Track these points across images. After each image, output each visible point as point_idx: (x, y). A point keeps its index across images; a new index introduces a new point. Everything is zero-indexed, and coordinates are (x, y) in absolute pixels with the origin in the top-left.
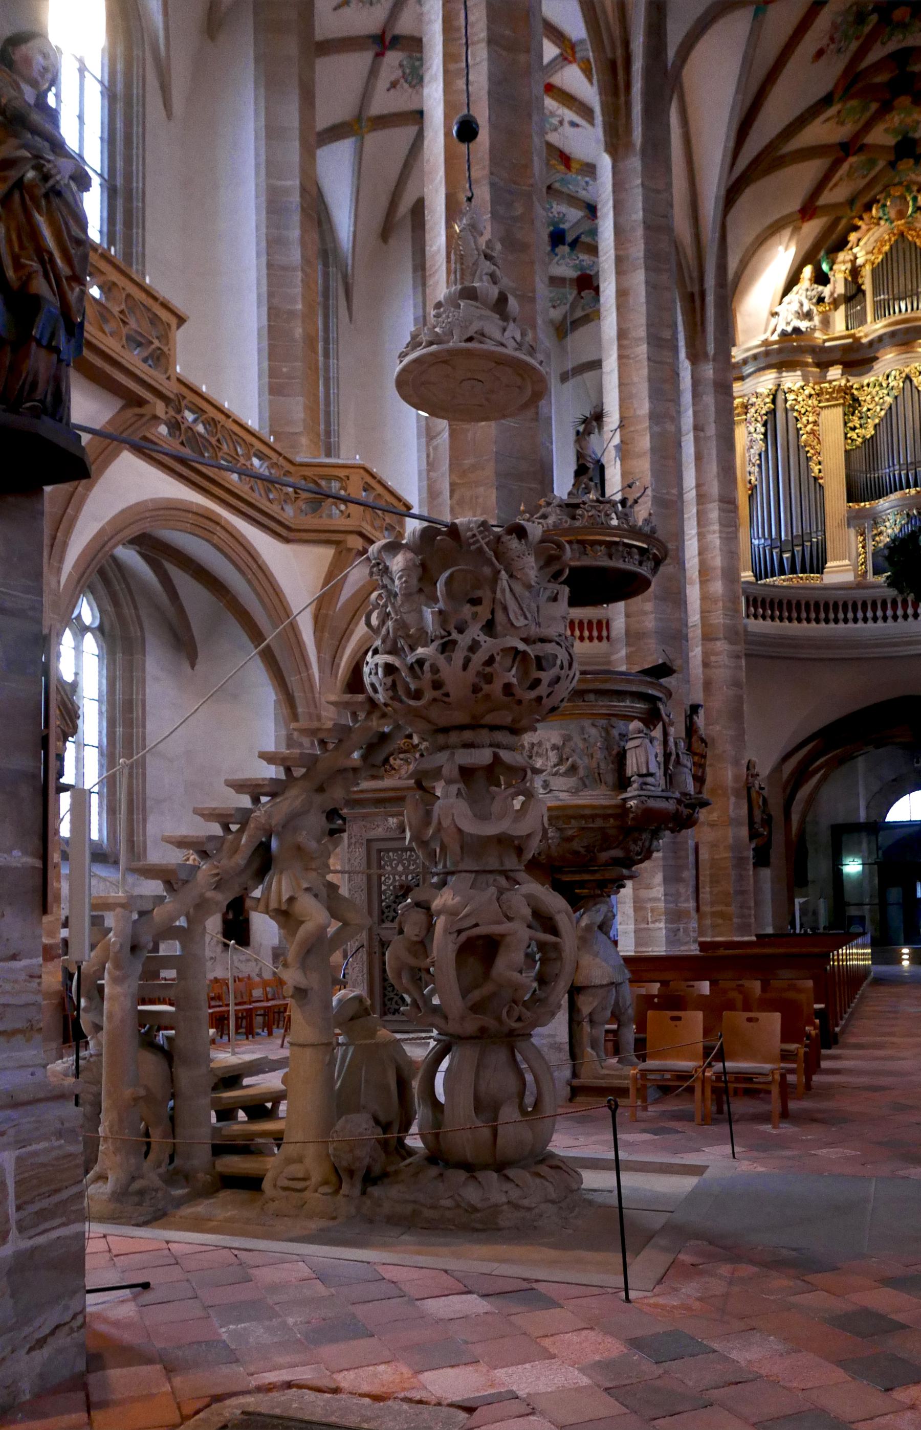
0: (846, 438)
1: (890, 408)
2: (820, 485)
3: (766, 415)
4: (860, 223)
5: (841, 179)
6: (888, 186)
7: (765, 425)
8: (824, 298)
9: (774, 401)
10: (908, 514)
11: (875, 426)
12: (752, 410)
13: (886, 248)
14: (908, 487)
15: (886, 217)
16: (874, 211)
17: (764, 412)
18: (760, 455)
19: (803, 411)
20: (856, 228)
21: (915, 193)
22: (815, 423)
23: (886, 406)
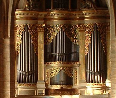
1: (56, 36)
3: (22, 32)
7: (22, 36)
9: (25, 29)
11: (52, 39)
12: (18, 30)
14: (60, 61)
17: (22, 31)
18: (20, 44)
23: (55, 35)
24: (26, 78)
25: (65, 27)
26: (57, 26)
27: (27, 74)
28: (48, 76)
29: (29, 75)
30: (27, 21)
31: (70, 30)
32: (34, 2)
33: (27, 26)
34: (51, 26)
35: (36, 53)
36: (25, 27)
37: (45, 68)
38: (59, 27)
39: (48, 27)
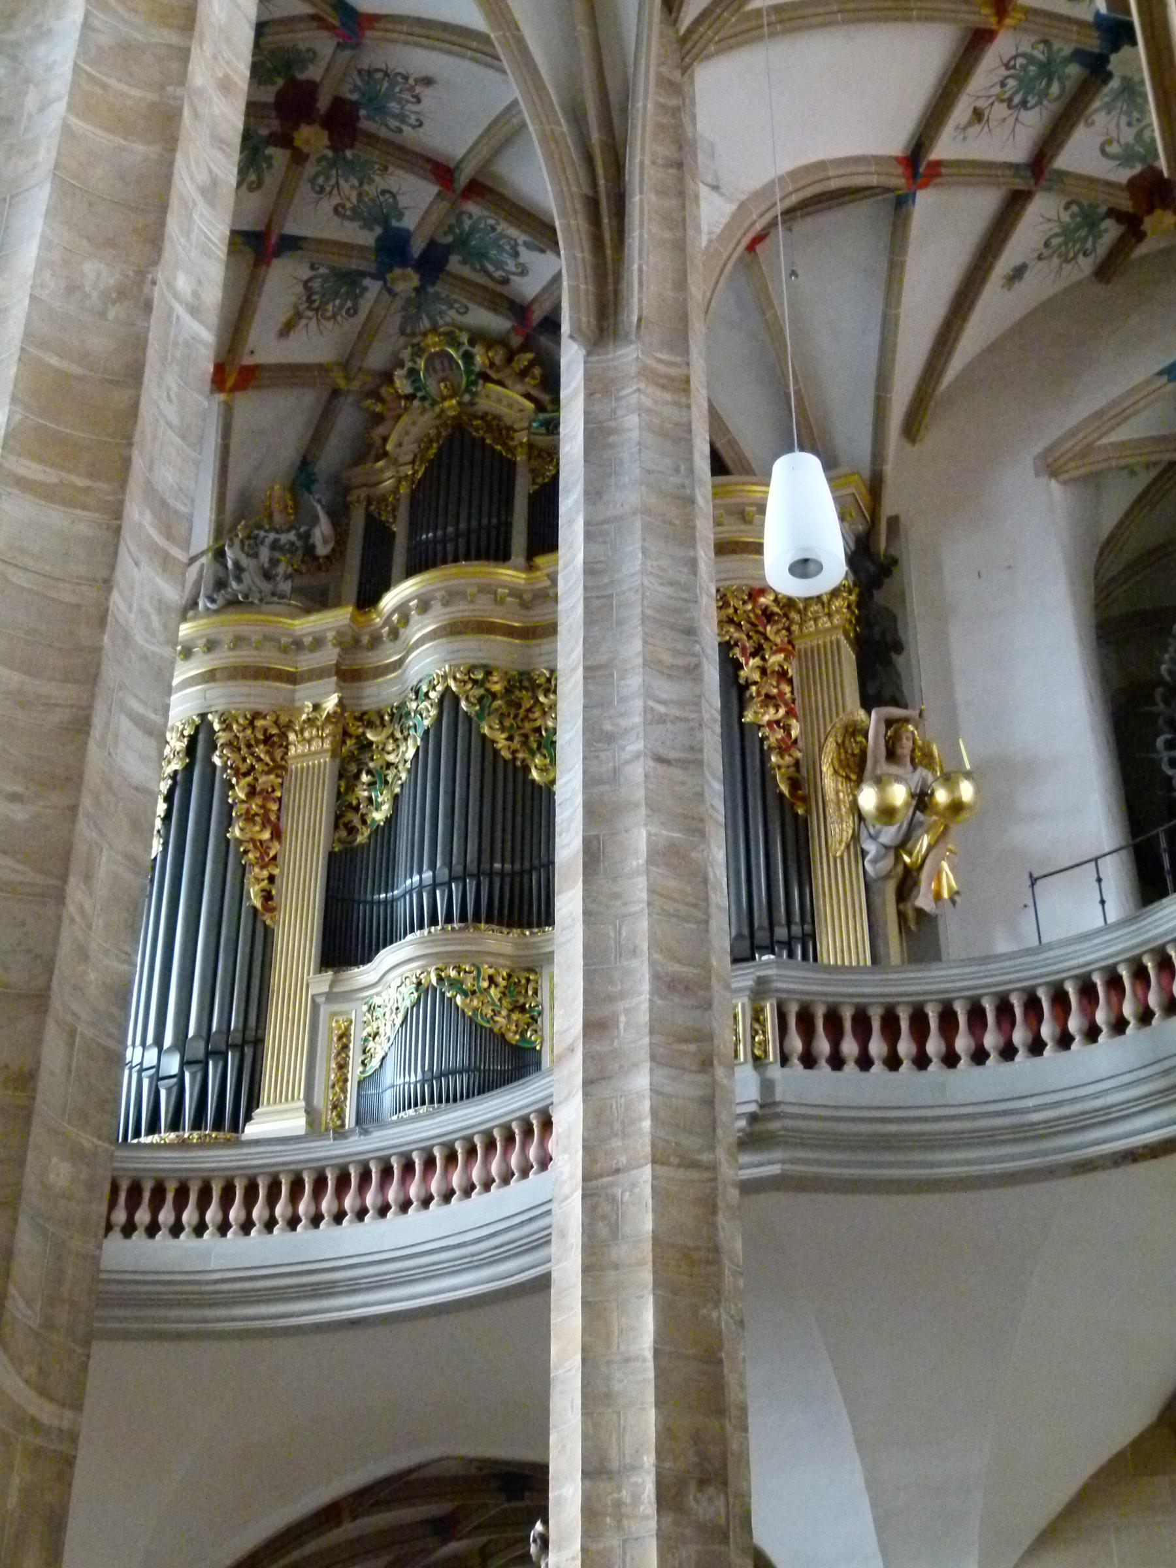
0: (336, 827)
1: (417, 754)
2: (266, 927)
4: (379, 408)
5: (298, 315)
6: (413, 335)
8: (313, 547)
9: (191, 750)
10: (419, 984)
13: (433, 451)
15: (419, 394)
16: (398, 383)
19: (243, 768)
20: (378, 419)
21: (466, 347)
22: (267, 795)
23: (410, 754)
24: (163, 1094)
25: (475, 682)
26: (424, 689)
27: (172, 1065)
28: (342, 1066)
29: (184, 1064)
30: (209, 693)
31: (528, 704)
32: (256, 555)
33: (211, 724)
34: (392, 715)
35: (257, 903)
36: (193, 740)
37: (324, 1011)
38: (433, 695)
39: (370, 725)
